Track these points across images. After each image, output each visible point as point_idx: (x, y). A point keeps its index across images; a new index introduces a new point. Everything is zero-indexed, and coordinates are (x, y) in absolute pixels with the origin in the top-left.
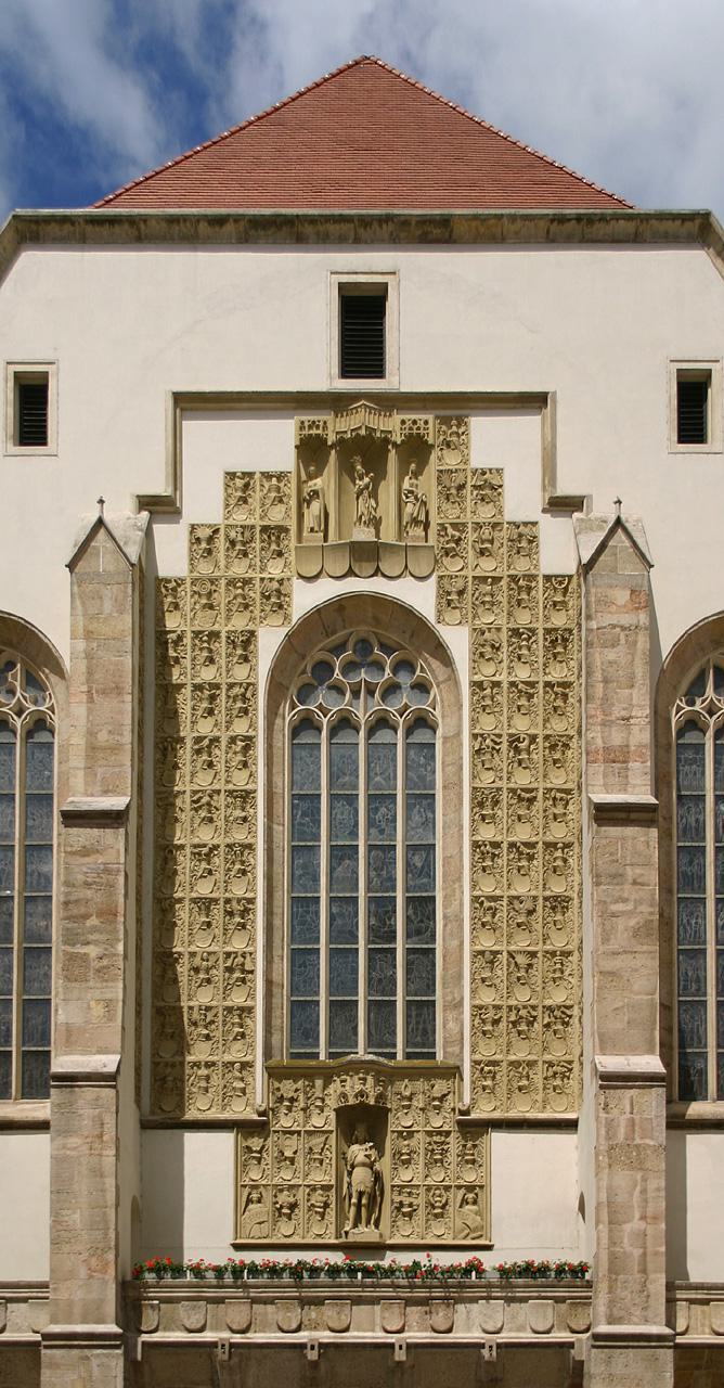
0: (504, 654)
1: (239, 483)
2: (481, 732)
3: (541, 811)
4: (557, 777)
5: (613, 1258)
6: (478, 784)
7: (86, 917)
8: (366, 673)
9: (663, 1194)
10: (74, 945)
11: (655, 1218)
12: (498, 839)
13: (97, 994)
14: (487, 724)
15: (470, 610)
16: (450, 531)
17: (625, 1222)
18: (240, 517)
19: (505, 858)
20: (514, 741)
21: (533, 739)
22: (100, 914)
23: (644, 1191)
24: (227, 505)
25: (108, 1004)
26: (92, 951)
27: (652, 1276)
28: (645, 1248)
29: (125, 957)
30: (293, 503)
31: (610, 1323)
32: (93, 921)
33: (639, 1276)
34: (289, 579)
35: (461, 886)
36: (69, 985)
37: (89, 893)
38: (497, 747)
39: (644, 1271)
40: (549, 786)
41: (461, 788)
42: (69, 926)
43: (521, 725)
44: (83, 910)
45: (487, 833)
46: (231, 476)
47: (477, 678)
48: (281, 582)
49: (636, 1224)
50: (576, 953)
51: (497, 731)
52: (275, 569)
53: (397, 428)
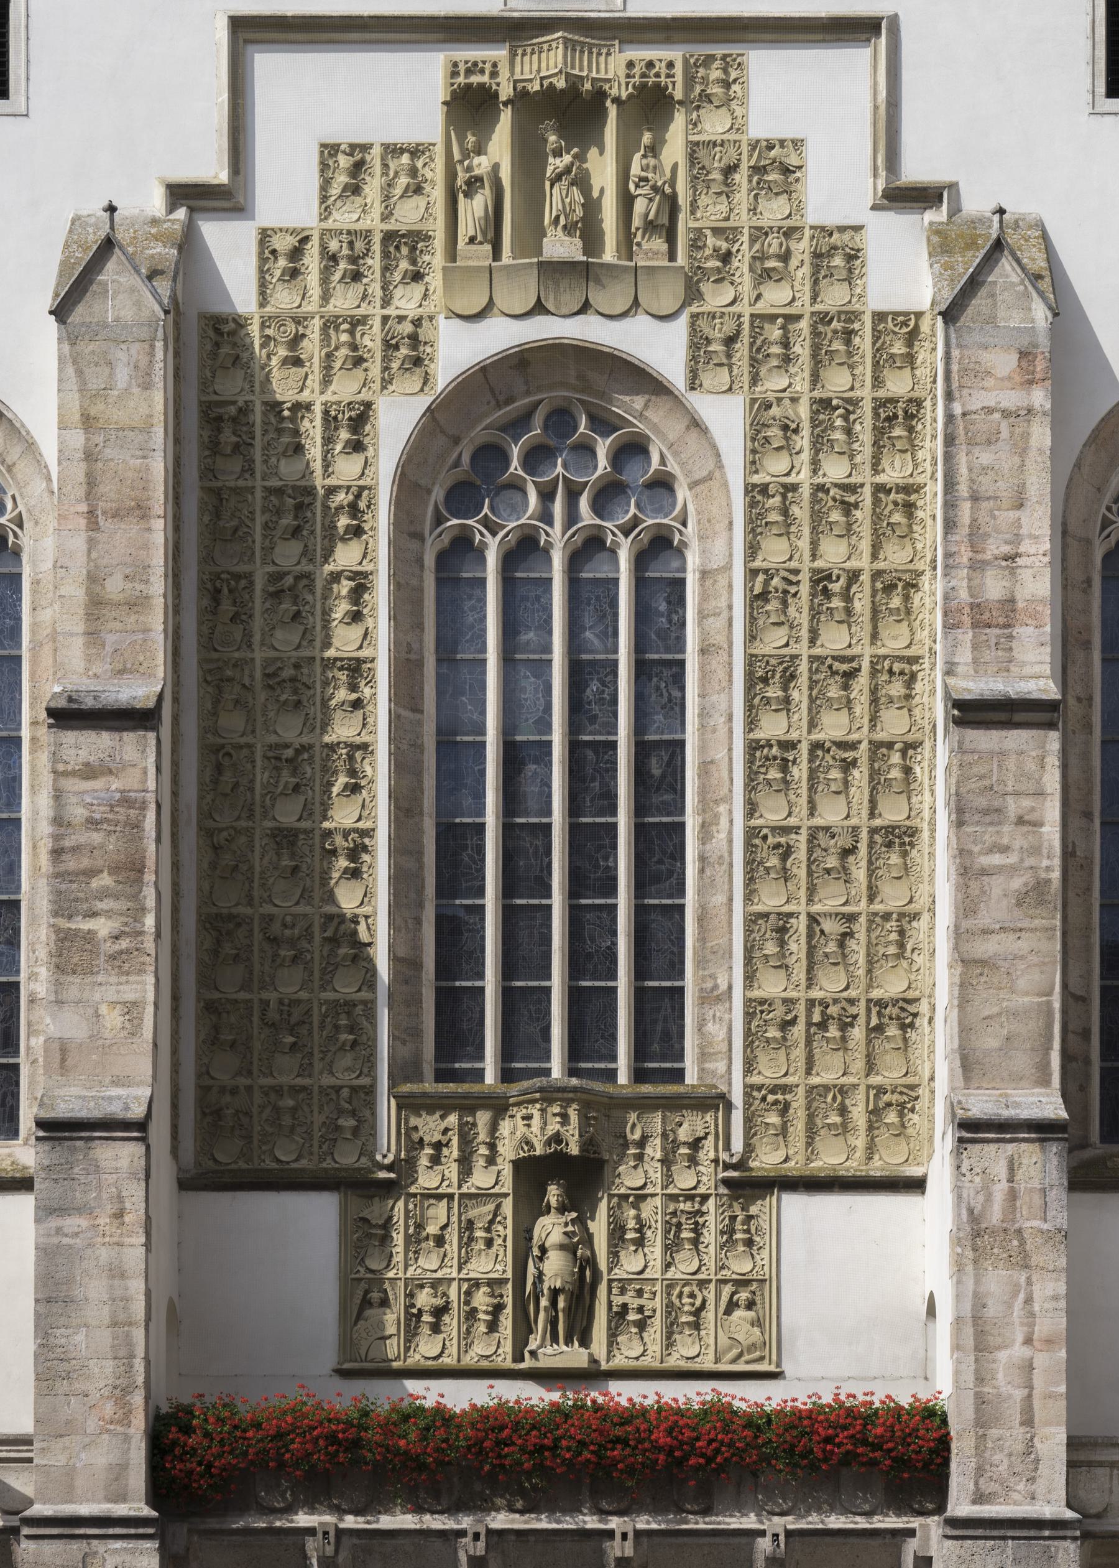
0: (803, 441)
1: (344, 161)
2: (765, 565)
3: (866, 691)
4: (895, 638)
5: (980, 1401)
6: (759, 649)
7: (91, 873)
8: (565, 466)
9: (1063, 1304)
10: (70, 917)
11: (1049, 1342)
12: (794, 736)
13: (111, 994)
14: (774, 551)
15: (746, 369)
16: (711, 241)
17: (998, 1348)
18: (345, 217)
19: (804, 765)
20: (821, 580)
21: (854, 576)
22: (114, 870)
23: (1029, 1300)
24: (324, 198)
25: (131, 1009)
26: (102, 927)
27: (1042, 1431)
28: (1031, 1388)
29: (158, 935)
30: (437, 194)
31: (974, 1502)
32: (105, 880)
33: (1022, 1430)
34: (431, 318)
35: (730, 812)
36: (63, 978)
37: (96, 837)
38: (793, 590)
39: (1028, 1421)
40: (882, 651)
41: (730, 655)
42: (63, 887)
43: (833, 553)
44: (85, 863)
45: (773, 727)
46: (329, 151)
47: (756, 479)
48: (417, 322)
49: (1018, 1351)
50: (925, 917)
51: (793, 564)
52: (407, 301)
53: (622, 72)
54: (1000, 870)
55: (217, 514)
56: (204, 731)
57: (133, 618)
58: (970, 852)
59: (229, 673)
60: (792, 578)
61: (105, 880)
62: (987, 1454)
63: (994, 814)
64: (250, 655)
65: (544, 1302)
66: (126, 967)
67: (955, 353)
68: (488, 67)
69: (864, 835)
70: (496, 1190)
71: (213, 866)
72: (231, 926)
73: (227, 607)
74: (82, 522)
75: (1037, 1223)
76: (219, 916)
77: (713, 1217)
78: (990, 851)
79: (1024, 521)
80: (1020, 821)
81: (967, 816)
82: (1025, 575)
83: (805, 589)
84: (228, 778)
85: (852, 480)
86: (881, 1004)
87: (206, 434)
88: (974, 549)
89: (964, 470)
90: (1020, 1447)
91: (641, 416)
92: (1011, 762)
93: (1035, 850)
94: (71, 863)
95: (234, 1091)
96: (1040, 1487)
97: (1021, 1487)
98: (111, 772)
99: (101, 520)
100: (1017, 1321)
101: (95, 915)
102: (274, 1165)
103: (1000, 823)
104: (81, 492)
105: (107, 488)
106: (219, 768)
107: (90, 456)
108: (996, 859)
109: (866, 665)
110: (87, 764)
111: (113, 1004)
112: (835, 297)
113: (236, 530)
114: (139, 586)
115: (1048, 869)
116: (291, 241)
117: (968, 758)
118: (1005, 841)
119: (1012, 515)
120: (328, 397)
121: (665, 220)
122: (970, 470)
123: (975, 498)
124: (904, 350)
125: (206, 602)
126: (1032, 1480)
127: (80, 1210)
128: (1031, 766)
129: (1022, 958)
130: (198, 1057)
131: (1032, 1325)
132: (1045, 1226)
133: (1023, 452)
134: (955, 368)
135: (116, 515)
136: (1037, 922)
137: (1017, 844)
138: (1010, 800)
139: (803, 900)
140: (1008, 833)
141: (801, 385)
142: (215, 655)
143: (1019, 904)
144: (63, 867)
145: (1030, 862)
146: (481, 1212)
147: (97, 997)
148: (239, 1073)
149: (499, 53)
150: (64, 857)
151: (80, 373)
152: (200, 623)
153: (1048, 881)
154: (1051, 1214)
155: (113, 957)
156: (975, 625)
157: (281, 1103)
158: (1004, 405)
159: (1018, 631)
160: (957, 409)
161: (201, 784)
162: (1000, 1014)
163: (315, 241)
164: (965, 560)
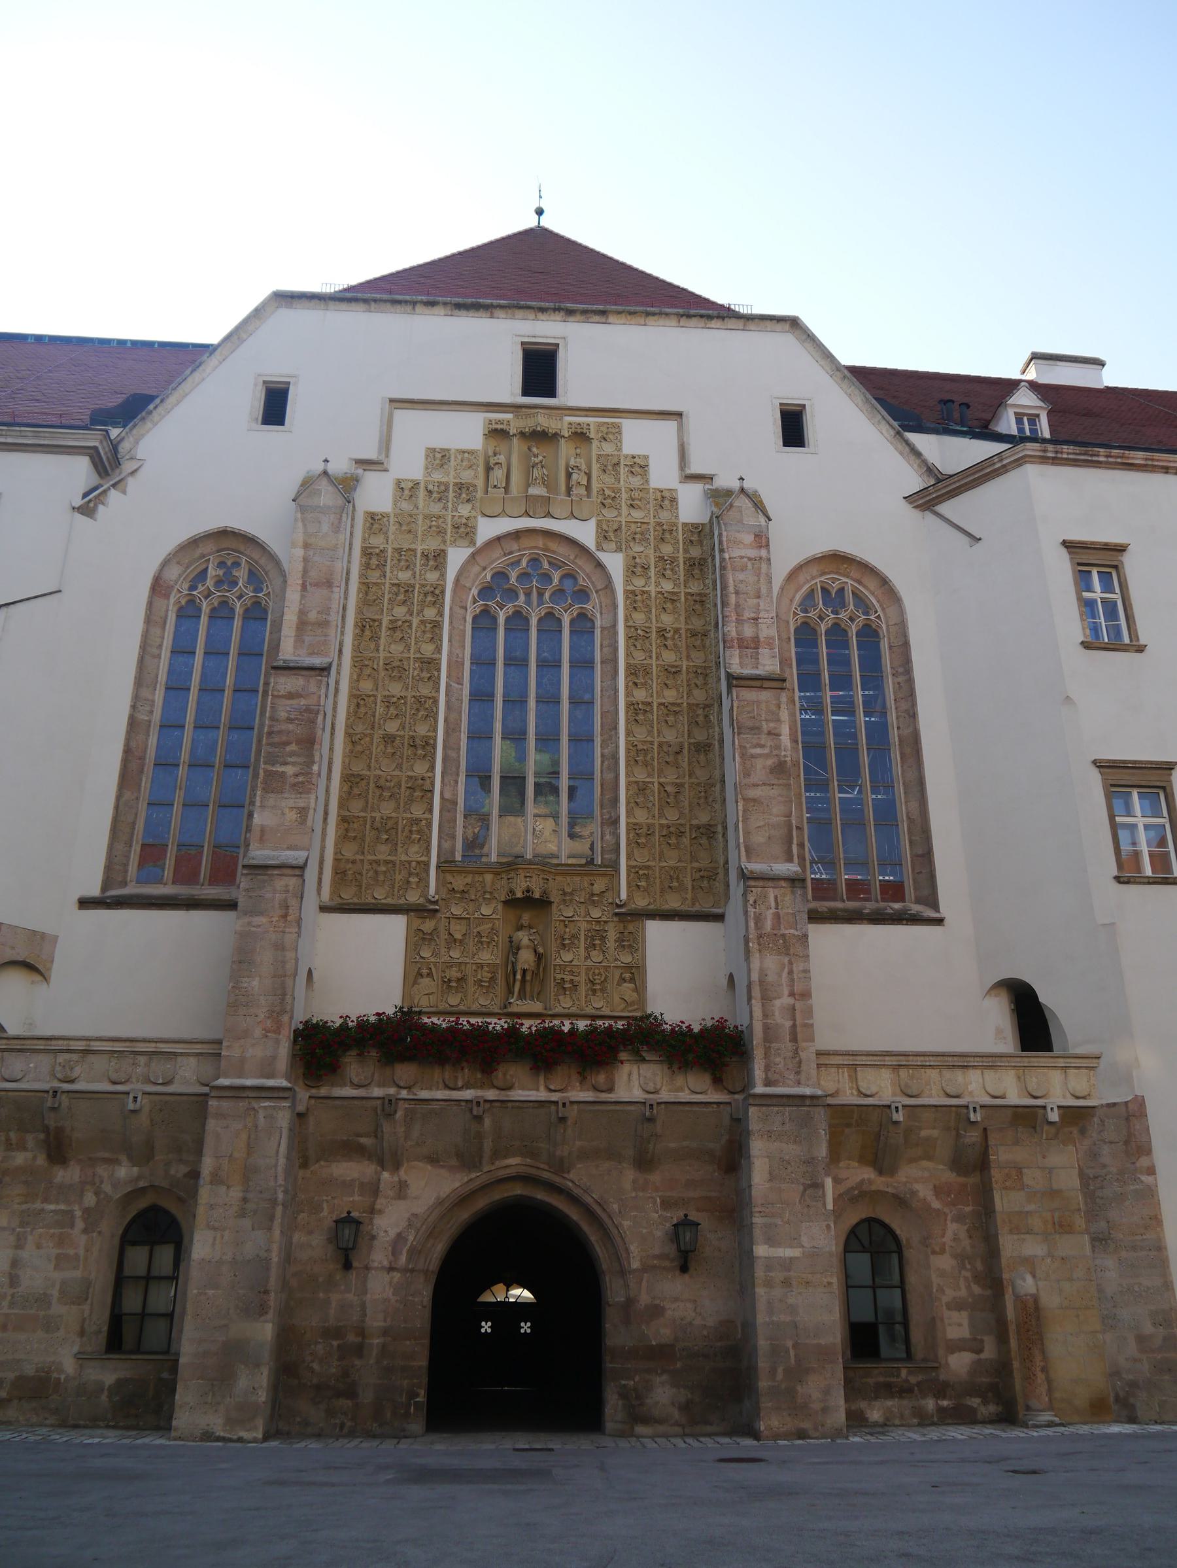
7: (288, 743)
13: (291, 803)
17: (775, 998)
18: (438, 476)
22: (298, 742)
23: (791, 972)
26: (290, 770)
28: (794, 1020)
30: (481, 470)
31: (766, 1085)
32: (293, 747)
33: (790, 1044)
37: (291, 727)
39: (794, 1039)
42: (271, 750)
44: (284, 738)
49: (786, 1000)
54: (761, 755)
55: (366, 594)
56: (351, 688)
57: (320, 631)
58: (745, 747)
59: (366, 663)
61: (293, 747)
63: (755, 729)
64: (377, 655)
65: (519, 977)
67: (724, 533)
69: (686, 746)
73: (368, 633)
74: (299, 588)
75: (792, 931)
76: (352, 775)
77: (612, 935)
80: (769, 733)
81: (743, 730)
83: (654, 635)
84: (362, 710)
86: (698, 827)
87: (363, 560)
89: (731, 581)
90: (790, 1054)
91: (574, 563)
92: (763, 706)
93: (778, 747)
94: (276, 739)
95: (354, 862)
96: (803, 1077)
97: (791, 1077)
99: (308, 587)
101: (286, 764)
102: (373, 901)
104: (300, 575)
105: (313, 574)
106: (358, 705)
107: (305, 560)
108: (758, 751)
109: (684, 668)
111: (291, 809)
112: (664, 516)
115: (785, 756)
116: (411, 485)
117: (742, 703)
118: (762, 742)
119: (755, 601)
122: (734, 581)
123: (737, 593)
124: (697, 539)
125: (357, 631)
126: (798, 1073)
127: (261, 914)
128: (774, 708)
129: (774, 798)
130: (336, 844)
132: (796, 933)
133: (759, 575)
134: (724, 539)
135: (316, 585)
136: (781, 782)
137: (769, 744)
138: (764, 723)
139: (656, 776)
140: (764, 739)
141: (651, 552)
144: (271, 740)
145: (775, 752)
146: (485, 928)
147: (283, 804)
149: (509, 416)
150: (273, 735)
151: (305, 525)
152: (354, 640)
159: (760, 650)
160: (726, 556)
161: (348, 712)
163: (422, 486)
164: (734, 618)
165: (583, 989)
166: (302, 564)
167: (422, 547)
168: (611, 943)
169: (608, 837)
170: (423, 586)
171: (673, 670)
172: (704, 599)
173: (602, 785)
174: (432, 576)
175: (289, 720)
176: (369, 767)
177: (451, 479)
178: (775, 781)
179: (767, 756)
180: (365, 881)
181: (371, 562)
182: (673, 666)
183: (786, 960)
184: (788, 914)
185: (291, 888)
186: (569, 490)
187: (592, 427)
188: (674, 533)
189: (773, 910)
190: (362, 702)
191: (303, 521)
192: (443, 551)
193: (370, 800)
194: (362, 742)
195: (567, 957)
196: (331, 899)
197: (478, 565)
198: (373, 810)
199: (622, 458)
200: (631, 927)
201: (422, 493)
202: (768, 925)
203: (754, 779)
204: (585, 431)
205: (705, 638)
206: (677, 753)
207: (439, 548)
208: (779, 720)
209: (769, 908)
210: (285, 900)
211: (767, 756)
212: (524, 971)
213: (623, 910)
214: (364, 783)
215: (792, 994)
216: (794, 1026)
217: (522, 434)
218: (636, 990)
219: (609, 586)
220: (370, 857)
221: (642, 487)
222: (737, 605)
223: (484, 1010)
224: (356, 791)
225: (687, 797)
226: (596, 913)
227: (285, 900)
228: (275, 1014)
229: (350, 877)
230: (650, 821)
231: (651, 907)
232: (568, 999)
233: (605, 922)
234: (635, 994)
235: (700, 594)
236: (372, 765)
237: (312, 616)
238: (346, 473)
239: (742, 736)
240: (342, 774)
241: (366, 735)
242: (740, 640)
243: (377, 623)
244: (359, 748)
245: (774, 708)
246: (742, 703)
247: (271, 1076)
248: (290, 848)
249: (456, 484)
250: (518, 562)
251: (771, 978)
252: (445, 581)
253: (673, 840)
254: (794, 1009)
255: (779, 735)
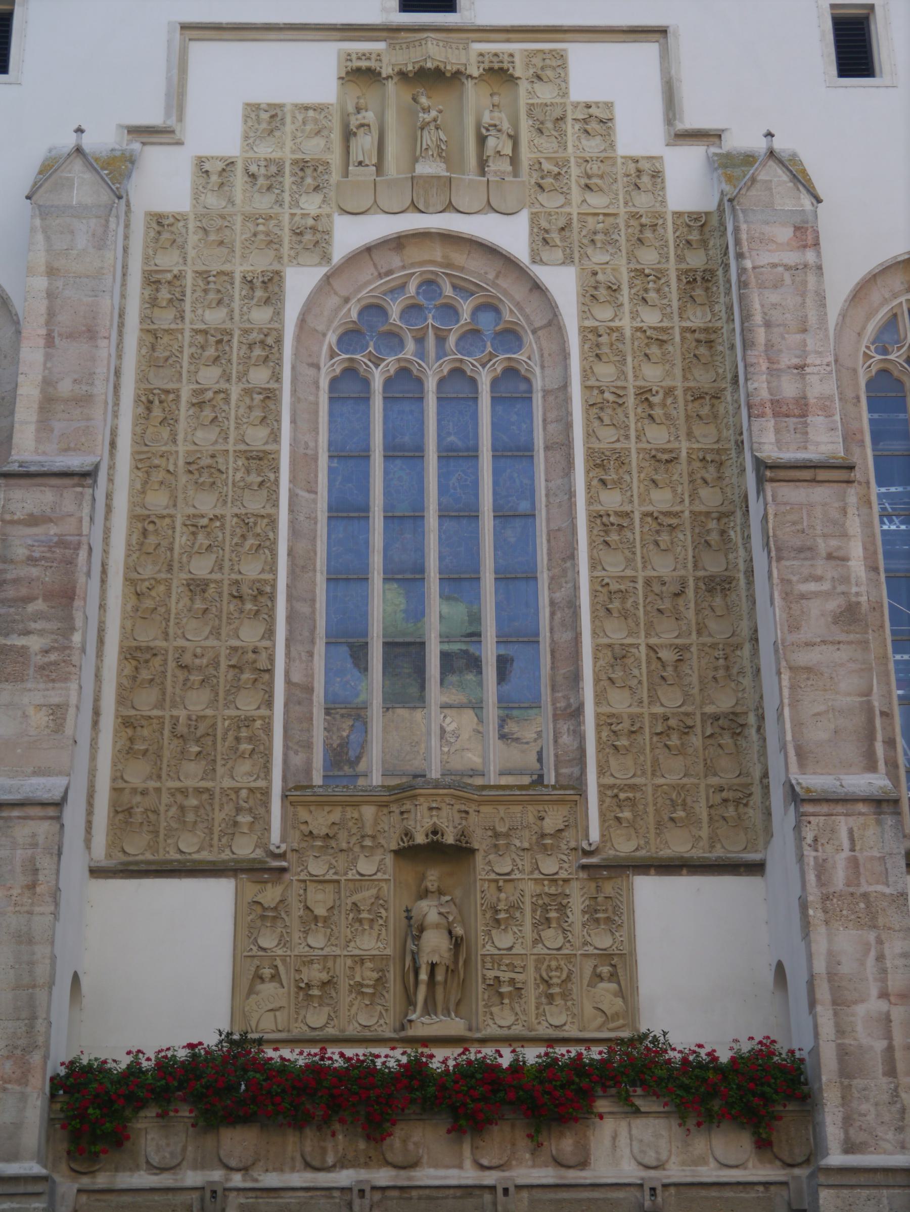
17: (855, 1002)
18: (265, 150)
22: (48, 596)
23: (880, 958)
26: (34, 643)
28: (889, 1037)
30: (336, 136)
32: (39, 605)
37: (34, 572)
39: (891, 1072)
44: (24, 591)
48: (316, 218)
49: (874, 1005)
54: (817, 594)
55: (153, 348)
56: (133, 504)
58: (789, 582)
59: (156, 462)
60: (621, 393)
61: (39, 605)
62: (854, 1104)
63: (806, 551)
64: (174, 448)
65: (424, 976)
66: (53, 676)
67: (744, 227)
68: (374, 56)
69: (691, 583)
70: (379, 876)
71: (136, 609)
72: (148, 656)
73: (157, 412)
74: (42, 342)
75: (880, 888)
76: (138, 648)
77: (577, 902)
78: (806, 580)
79: (809, 342)
80: (830, 557)
82: (813, 380)
83: (631, 401)
84: (152, 540)
85: (664, 324)
86: (716, 718)
87: (147, 293)
88: (770, 360)
89: (757, 305)
90: (885, 1097)
91: (495, 285)
93: (845, 579)
95: (144, 793)
97: (890, 1136)
98: (50, 520)
99: (57, 340)
100: (871, 978)
101: (27, 633)
102: (178, 856)
103: (813, 558)
104: (42, 320)
106: (145, 533)
107: (51, 295)
108: (812, 587)
109: (684, 454)
110: (31, 515)
111: (39, 707)
112: (642, 201)
113: (167, 359)
114: (84, 388)
116: (220, 165)
117: (782, 508)
118: (819, 572)
119: (799, 337)
120: (246, 267)
121: (508, 151)
122: (762, 306)
123: (768, 325)
124: (698, 237)
125: (141, 410)
128: (835, 514)
130: (114, 764)
131: (884, 980)
132: (888, 891)
133: (803, 295)
134: (744, 236)
135: (71, 336)
136: (852, 637)
137: (829, 575)
138: (820, 541)
139: (643, 634)
140: (821, 567)
141: (621, 262)
142: (146, 449)
143: (835, 623)
145: (840, 589)
146: (365, 896)
147: (26, 700)
148: (150, 778)
149: (380, 46)
151: (48, 238)
152: (135, 425)
153: (859, 603)
154: (891, 879)
155: (42, 668)
156: (776, 415)
157: (186, 803)
158: (785, 261)
159: (809, 419)
160: (748, 264)
161: (129, 545)
162: (827, 712)
163: (240, 167)
164: (764, 368)
165: (532, 994)
166: (45, 302)
167: (242, 269)
168: (576, 916)
169: (565, 739)
170: (246, 332)
171: (666, 457)
172: (713, 337)
173: (553, 652)
174: (261, 316)
175: (32, 560)
176: (166, 634)
177: (287, 155)
178: (843, 637)
179: (827, 595)
180: (163, 824)
181: (160, 295)
182: (664, 451)
183: (872, 936)
184: (872, 858)
185: (41, 840)
186: (482, 165)
187: (517, 59)
188: (660, 230)
189: (846, 853)
190: (151, 528)
191: (45, 230)
192: (277, 273)
193: (169, 690)
194: (153, 593)
195: (504, 940)
196: (109, 856)
197: (336, 293)
198: (174, 705)
199: (569, 109)
200: (608, 888)
201: (239, 180)
202: (839, 878)
203: (806, 634)
204: (505, 66)
205: (716, 402)
206: (677, 595)
207: (271, 268)
208: (844, 535)
209: (839, 849)
210: (32, 860)
211: (827, 595)
212: (433, 966)
213: (594, 860)
214: (157, 661)
215: (884, 995)
216: (890, 1049)
217: (403, 75)
218: (620, 993)
219: (554, 322)
220: (172, 784)
221: (603, 155)
222: (769, 345)
223: (367, 1034)
224: (145, 675)
225: (695, 667)
226: (549, 866)
227: (32, 860)
228: (18, 1052)
229: (138, 818)
230: (635, 710)
231: (642, 853)
232: (507, 1012)
233: (566, 881)
234: (619, 1001)
235: (706, 330)
236: (171, 631)
237: (65, 387)
238: (112, 150)
239: (784, 563)
240: (121, 647)
241: (158, 582)
242: (776, 403)
243: (171, 396)
244: (148, 603)
245: (835, 514)
246: (782, 508)
247: (14, 1157)
248: (38, 772)
249: (295, 162)
250: (403, 287)
251: (847, 967)
252: (282, 322)
253: (674, 741)
254: (888, 1020)
255: (845, 559)
